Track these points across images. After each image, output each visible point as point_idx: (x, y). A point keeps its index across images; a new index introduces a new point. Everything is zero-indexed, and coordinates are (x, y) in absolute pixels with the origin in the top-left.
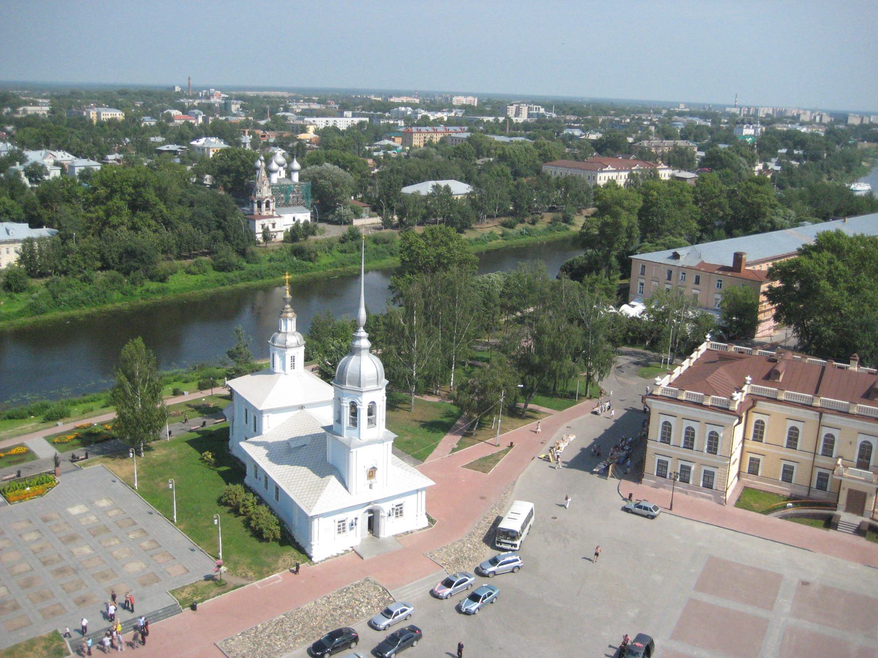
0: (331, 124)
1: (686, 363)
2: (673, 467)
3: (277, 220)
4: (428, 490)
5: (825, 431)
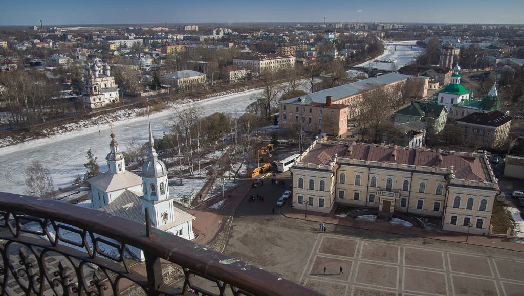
0: (123, 44)
1: (308, 151)
2: (305, 199)
3: (101, 96)
4: (193, 220)
5: (372, 176)
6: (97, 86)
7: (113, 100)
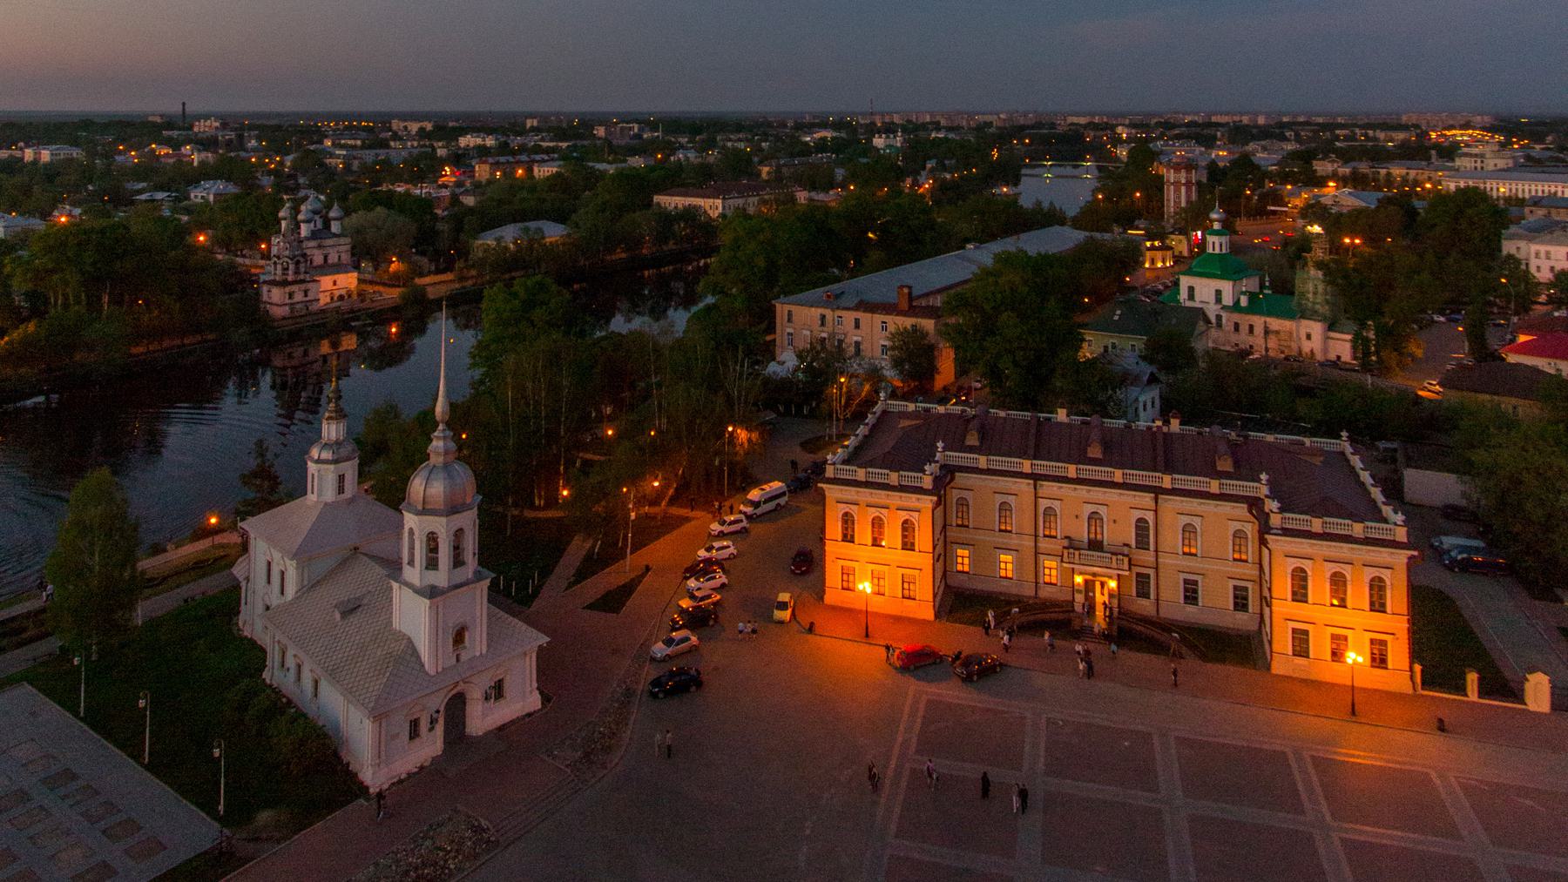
6: (302, 260)
7: (341, 298)
